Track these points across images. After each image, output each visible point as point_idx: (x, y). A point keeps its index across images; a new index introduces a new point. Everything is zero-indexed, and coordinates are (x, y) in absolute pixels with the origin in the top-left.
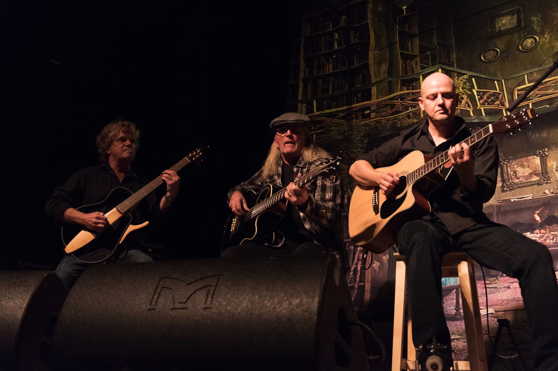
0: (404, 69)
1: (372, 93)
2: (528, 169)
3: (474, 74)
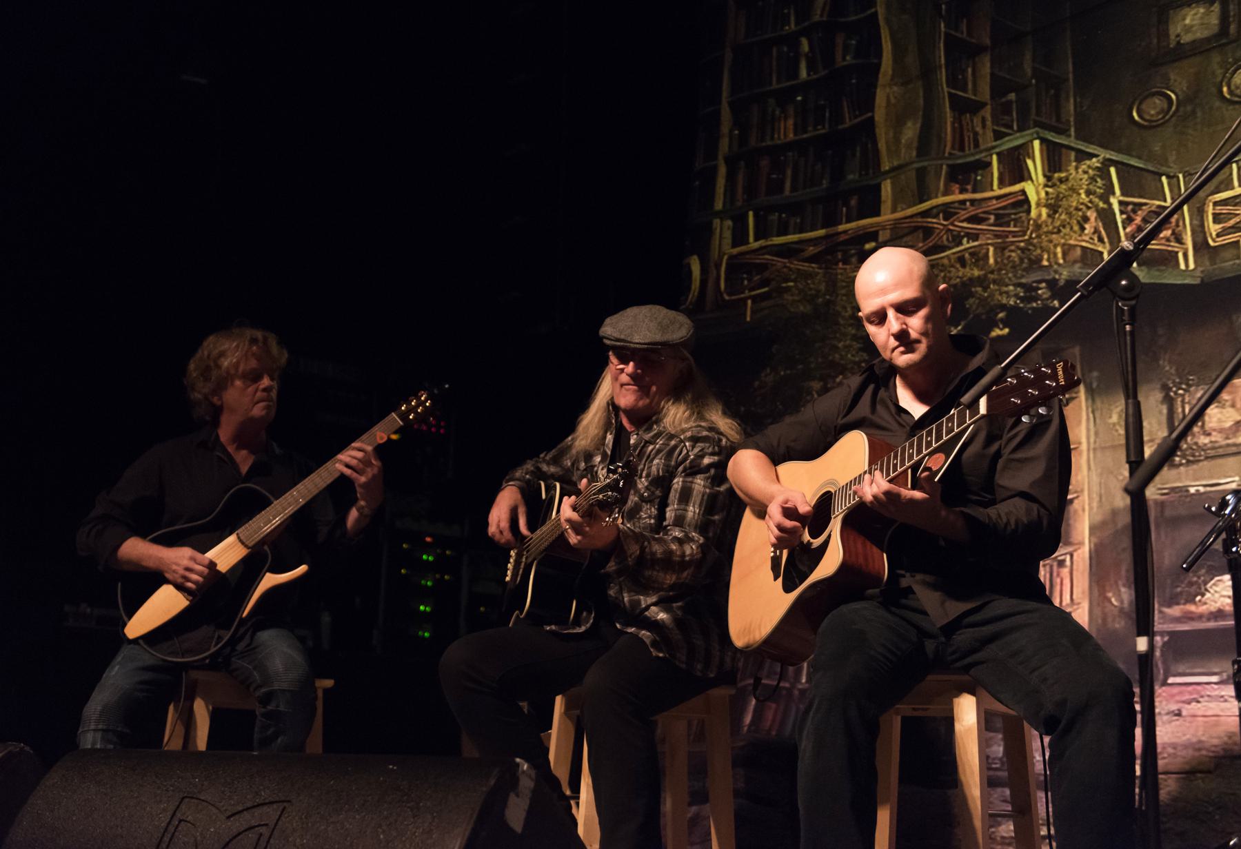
0: (957, 136)
1: (883, 198)
2: (1231, 410)
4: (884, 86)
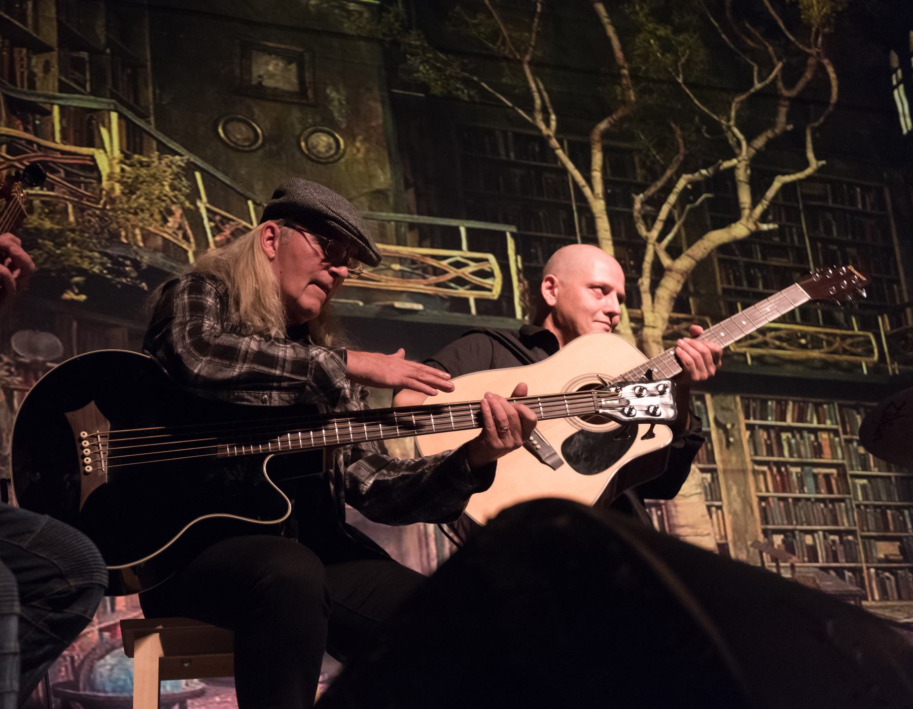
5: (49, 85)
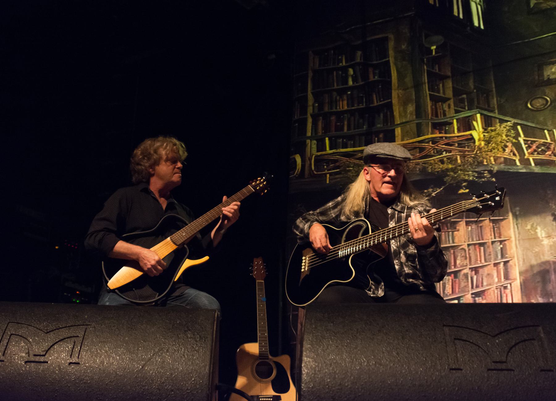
0: (434, 112)
3: (519, 122)
4: (395, 90)
5: (451, 113)
